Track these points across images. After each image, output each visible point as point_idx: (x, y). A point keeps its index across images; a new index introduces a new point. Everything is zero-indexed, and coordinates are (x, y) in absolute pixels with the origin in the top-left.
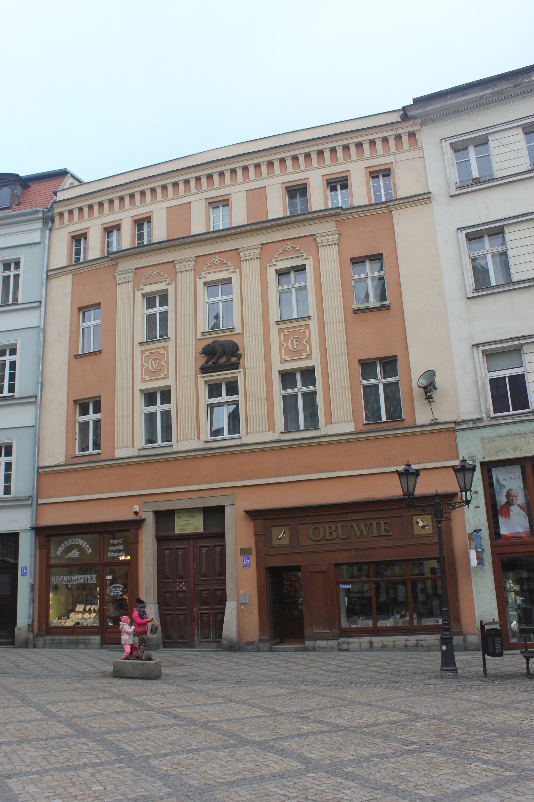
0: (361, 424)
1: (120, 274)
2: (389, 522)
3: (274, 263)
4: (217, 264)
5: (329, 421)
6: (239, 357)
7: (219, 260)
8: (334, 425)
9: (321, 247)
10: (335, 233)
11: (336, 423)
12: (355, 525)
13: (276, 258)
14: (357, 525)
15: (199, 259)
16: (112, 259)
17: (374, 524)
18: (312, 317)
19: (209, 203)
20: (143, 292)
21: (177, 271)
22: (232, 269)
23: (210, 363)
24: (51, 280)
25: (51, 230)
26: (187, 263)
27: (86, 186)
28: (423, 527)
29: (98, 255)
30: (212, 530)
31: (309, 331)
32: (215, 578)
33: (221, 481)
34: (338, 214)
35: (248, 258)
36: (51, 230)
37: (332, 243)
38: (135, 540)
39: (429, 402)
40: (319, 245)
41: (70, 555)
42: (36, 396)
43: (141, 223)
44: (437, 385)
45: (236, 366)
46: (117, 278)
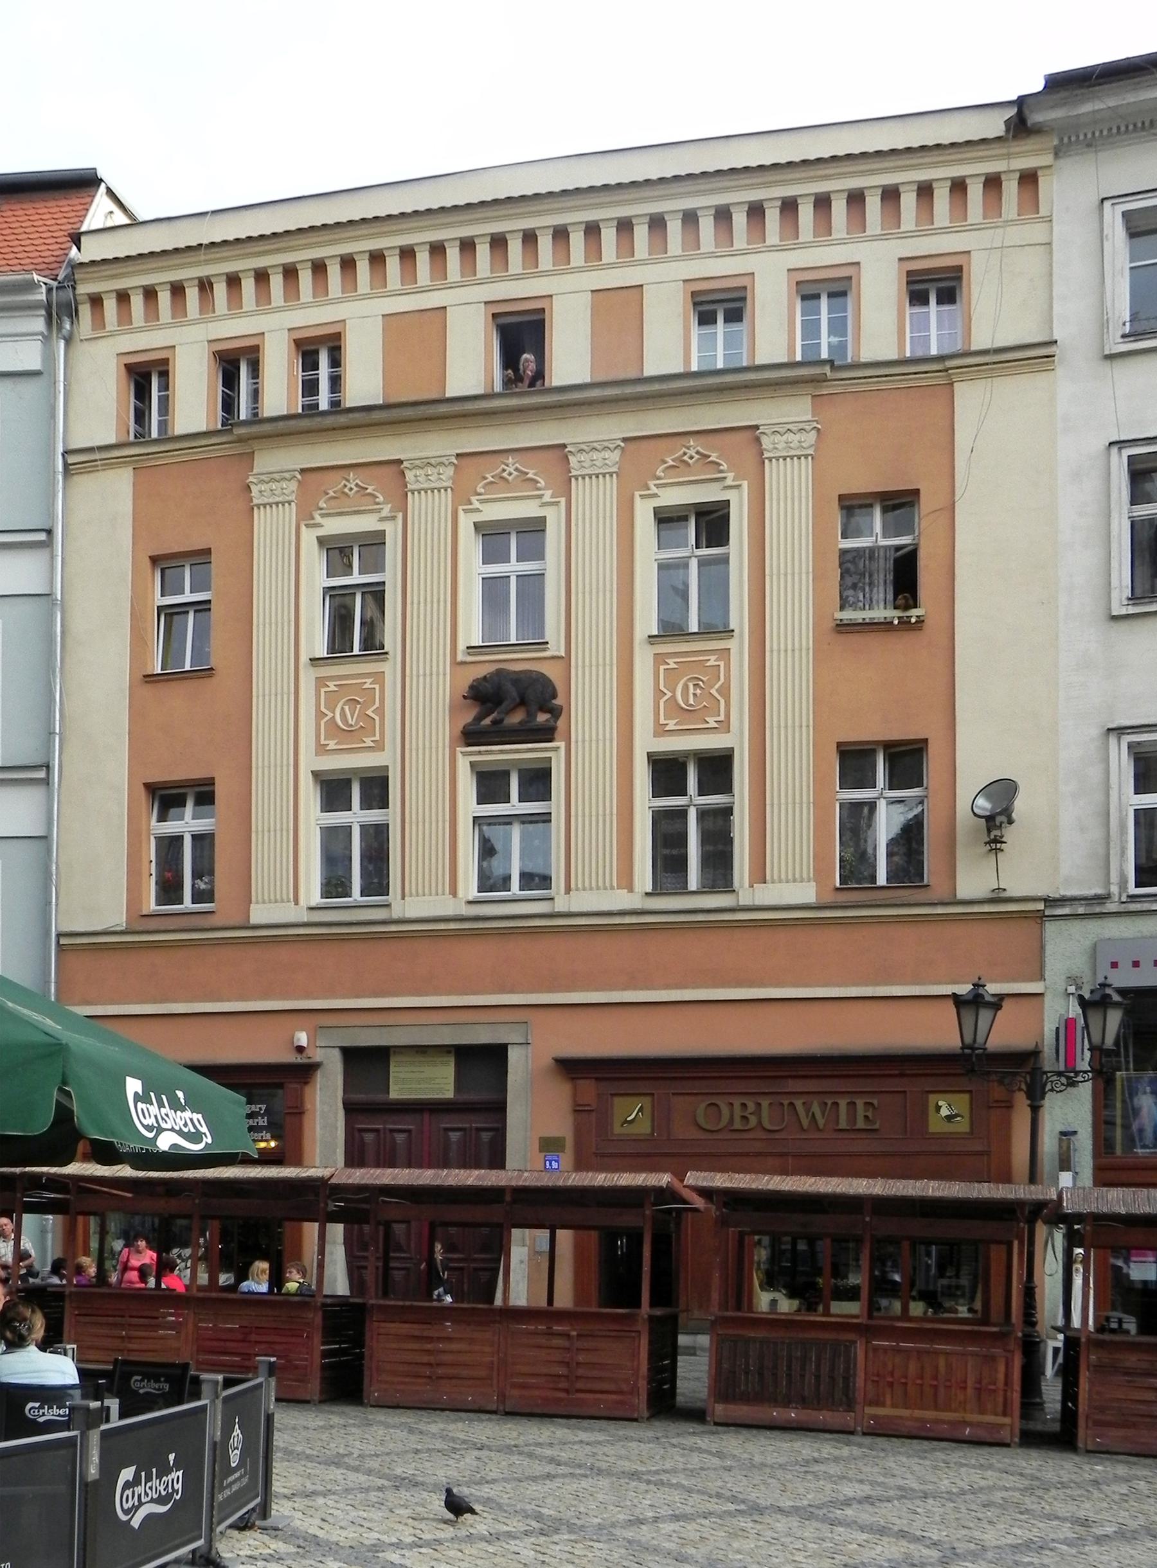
2: (875, 1102)
5: (760, 875)
8: (770, 885)
12: (799, 1103)
17: (843, 1103)
28: (949, 1118)
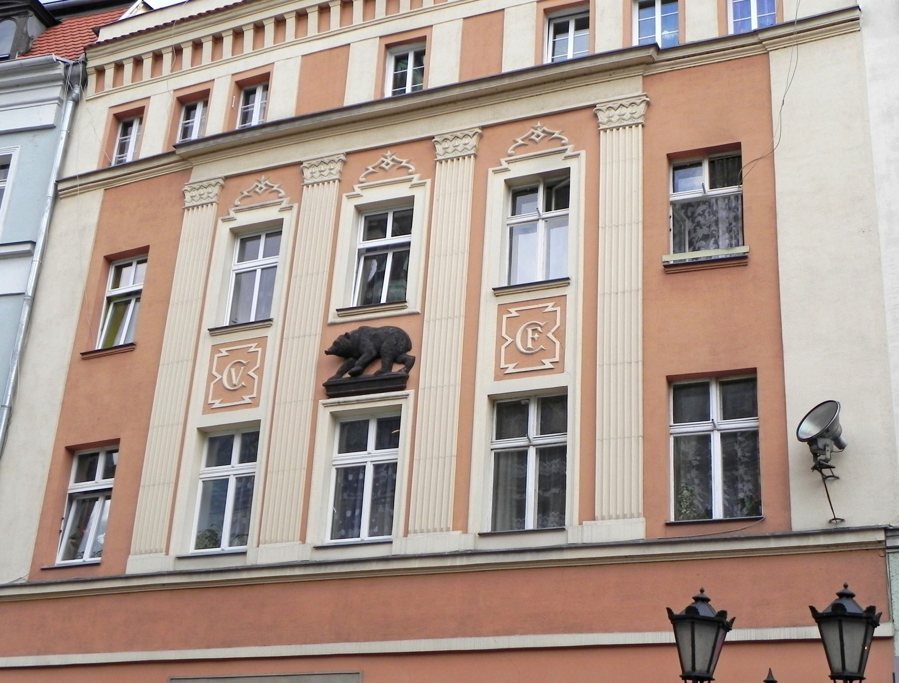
0: (663, 522)
1: (193, 189)
3: (505, 165)
4: (387, 167)
5: (589, 513)
6: (410, 363)
7: (393, 160)
8: (599, 522)
9: (605, 130)
10: (638, 102)
11: (603, 518)
13: (510, 155)
15: (352, 159)
16: (184, 159)
18: (572, 282)
19: (388, 47)
20: (234, 225)
21: (306, 182)
22: (416, 179)
23: (347, 375)
24: (63, 201)
25: (77, 103)
26: (327, 167)
27: (157, 14)
29: (159, 151)
31: (564, 312)
34: (650, 60)
35: (451, 156)
36: (77, 103)
37: (630, 122)
39: (825, 478)
40: (602, 127)
43: (249, 87)
44: (843, 438)
45: (399, 383)
46: (188, 195)
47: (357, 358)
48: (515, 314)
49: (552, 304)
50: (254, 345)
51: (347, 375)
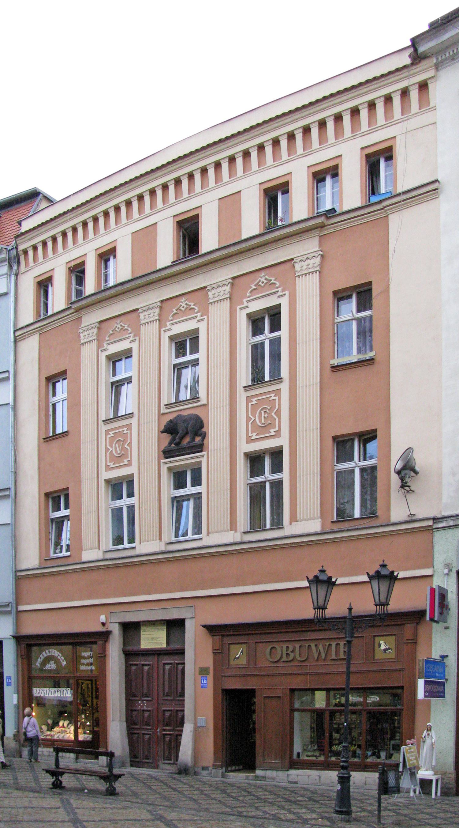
8: (299, 523)
12: (313, 645)
14: (316, 645)
17: (334, 644)
28: (385, 650)
30: (174, 646)
32: (178, 698)
33: (182, 590)
38: (102, 654)
41: (48, 667)
42: (10, 488)
47: (177, 434)
48: (255, 402)
49: (274, 395)
50: (126, 429)
51: (173, 445)
